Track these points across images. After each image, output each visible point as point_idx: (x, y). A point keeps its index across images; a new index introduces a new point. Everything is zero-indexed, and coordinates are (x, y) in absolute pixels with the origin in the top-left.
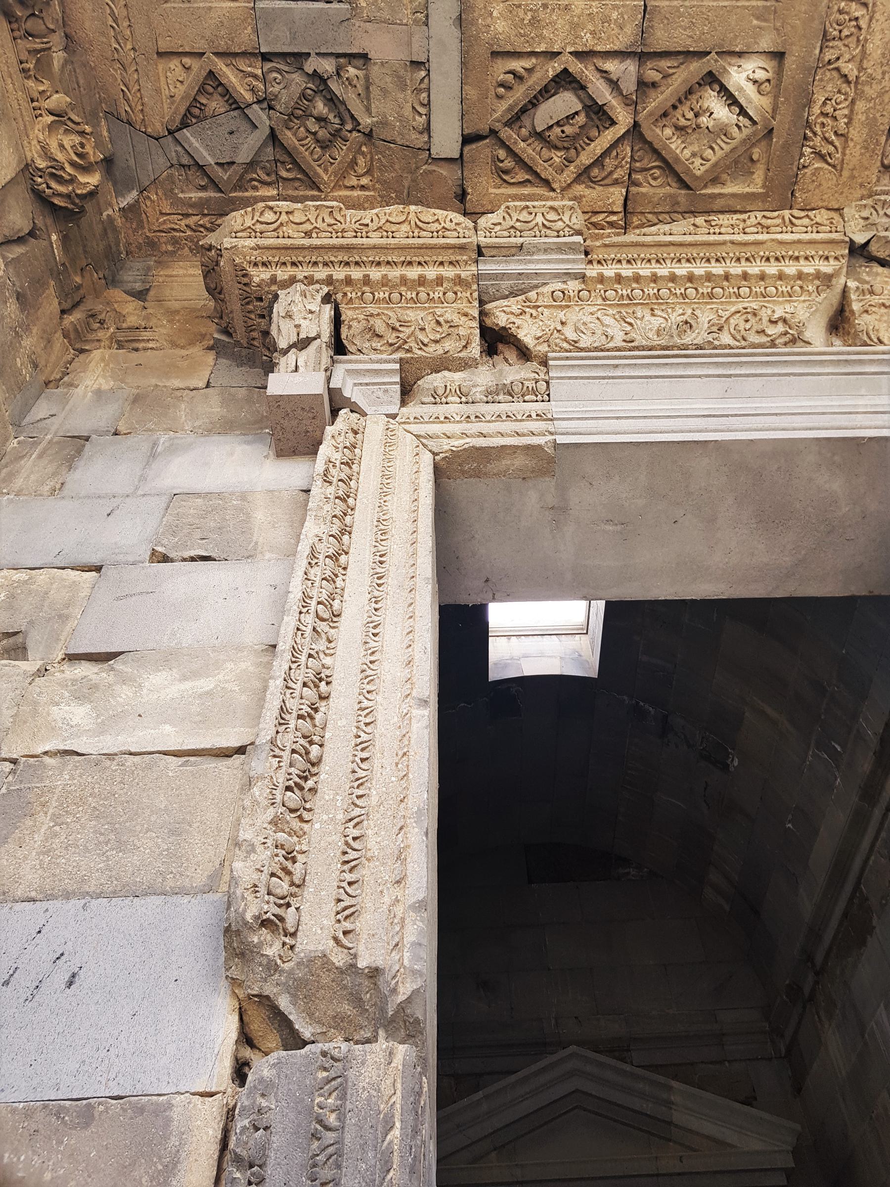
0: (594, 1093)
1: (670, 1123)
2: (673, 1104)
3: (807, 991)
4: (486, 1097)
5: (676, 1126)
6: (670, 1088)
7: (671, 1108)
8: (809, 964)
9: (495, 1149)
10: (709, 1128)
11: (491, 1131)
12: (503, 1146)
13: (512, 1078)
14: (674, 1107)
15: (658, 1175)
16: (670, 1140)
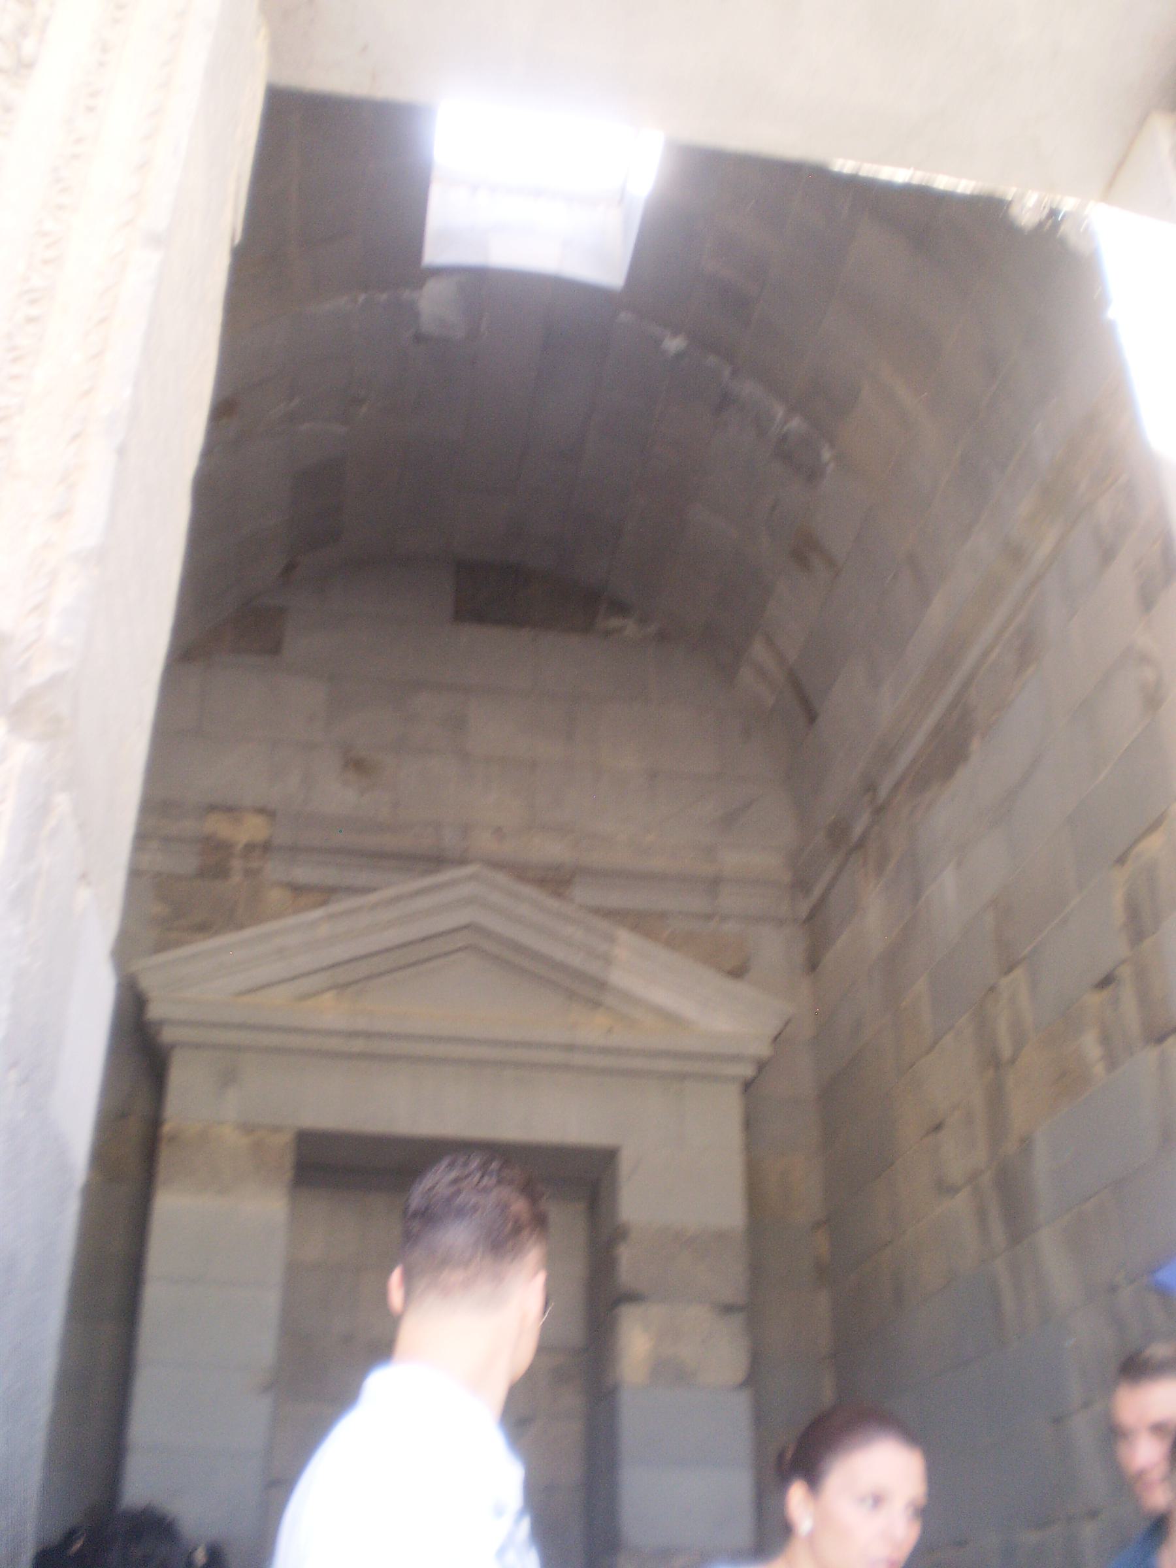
10: (661, 996)
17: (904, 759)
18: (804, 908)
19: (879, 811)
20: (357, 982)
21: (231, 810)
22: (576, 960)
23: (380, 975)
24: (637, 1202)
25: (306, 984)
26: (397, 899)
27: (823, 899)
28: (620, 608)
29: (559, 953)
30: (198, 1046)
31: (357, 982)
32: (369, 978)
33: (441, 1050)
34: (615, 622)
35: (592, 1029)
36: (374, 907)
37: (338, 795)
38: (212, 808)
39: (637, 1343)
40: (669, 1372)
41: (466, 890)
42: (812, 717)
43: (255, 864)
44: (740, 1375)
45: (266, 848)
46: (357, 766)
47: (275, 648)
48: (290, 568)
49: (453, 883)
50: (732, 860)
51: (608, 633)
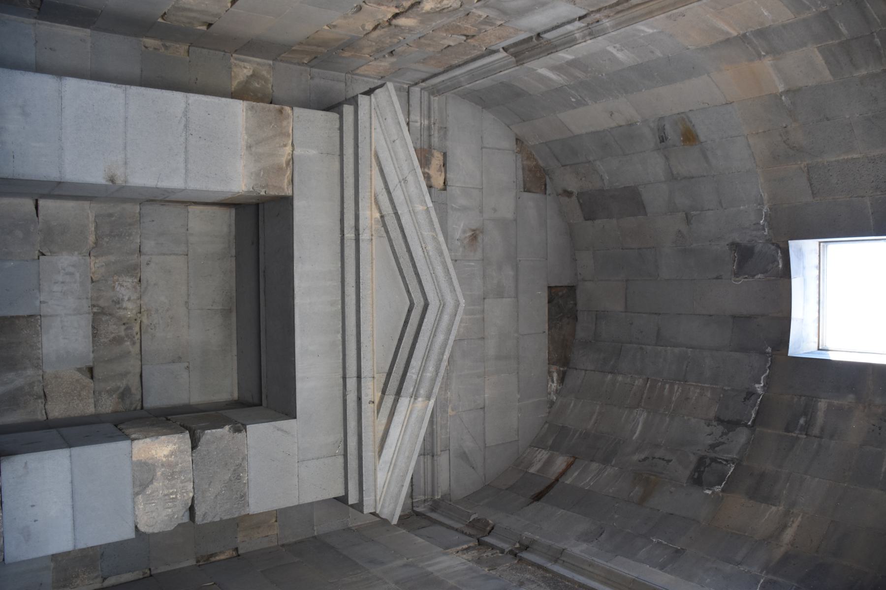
0: (426, 320)
1: (398, 393)
3: (488, 539)
5: (396, 401)
6: (428, 398)
8: (517, 545)
9: (382, 217)
11: (399, 212)
12: (384, 225)
13: (441, 238)
15: (359, 377)
17: (556, 568)
19: (514, 554)
20: (387, 232)
22: (412, 374)
24: (260, 434)
26: (441, 254)
28: (562, 379)
29: (415, 363)
30: (341, 129)
31: (387, 232)
32: (390, 240)
33: (351, 290)
34: (555, 376)
35: (371, 390)
36: (435, 238)
38: (445, 155)
39: (162, 449)
40: (144, 476)
42: (538, 497)
44: (142, 528)
46: (474, 237)
47: (527, 190)
48: (569, 194)
50: (443, 460)
51: (550, 373)
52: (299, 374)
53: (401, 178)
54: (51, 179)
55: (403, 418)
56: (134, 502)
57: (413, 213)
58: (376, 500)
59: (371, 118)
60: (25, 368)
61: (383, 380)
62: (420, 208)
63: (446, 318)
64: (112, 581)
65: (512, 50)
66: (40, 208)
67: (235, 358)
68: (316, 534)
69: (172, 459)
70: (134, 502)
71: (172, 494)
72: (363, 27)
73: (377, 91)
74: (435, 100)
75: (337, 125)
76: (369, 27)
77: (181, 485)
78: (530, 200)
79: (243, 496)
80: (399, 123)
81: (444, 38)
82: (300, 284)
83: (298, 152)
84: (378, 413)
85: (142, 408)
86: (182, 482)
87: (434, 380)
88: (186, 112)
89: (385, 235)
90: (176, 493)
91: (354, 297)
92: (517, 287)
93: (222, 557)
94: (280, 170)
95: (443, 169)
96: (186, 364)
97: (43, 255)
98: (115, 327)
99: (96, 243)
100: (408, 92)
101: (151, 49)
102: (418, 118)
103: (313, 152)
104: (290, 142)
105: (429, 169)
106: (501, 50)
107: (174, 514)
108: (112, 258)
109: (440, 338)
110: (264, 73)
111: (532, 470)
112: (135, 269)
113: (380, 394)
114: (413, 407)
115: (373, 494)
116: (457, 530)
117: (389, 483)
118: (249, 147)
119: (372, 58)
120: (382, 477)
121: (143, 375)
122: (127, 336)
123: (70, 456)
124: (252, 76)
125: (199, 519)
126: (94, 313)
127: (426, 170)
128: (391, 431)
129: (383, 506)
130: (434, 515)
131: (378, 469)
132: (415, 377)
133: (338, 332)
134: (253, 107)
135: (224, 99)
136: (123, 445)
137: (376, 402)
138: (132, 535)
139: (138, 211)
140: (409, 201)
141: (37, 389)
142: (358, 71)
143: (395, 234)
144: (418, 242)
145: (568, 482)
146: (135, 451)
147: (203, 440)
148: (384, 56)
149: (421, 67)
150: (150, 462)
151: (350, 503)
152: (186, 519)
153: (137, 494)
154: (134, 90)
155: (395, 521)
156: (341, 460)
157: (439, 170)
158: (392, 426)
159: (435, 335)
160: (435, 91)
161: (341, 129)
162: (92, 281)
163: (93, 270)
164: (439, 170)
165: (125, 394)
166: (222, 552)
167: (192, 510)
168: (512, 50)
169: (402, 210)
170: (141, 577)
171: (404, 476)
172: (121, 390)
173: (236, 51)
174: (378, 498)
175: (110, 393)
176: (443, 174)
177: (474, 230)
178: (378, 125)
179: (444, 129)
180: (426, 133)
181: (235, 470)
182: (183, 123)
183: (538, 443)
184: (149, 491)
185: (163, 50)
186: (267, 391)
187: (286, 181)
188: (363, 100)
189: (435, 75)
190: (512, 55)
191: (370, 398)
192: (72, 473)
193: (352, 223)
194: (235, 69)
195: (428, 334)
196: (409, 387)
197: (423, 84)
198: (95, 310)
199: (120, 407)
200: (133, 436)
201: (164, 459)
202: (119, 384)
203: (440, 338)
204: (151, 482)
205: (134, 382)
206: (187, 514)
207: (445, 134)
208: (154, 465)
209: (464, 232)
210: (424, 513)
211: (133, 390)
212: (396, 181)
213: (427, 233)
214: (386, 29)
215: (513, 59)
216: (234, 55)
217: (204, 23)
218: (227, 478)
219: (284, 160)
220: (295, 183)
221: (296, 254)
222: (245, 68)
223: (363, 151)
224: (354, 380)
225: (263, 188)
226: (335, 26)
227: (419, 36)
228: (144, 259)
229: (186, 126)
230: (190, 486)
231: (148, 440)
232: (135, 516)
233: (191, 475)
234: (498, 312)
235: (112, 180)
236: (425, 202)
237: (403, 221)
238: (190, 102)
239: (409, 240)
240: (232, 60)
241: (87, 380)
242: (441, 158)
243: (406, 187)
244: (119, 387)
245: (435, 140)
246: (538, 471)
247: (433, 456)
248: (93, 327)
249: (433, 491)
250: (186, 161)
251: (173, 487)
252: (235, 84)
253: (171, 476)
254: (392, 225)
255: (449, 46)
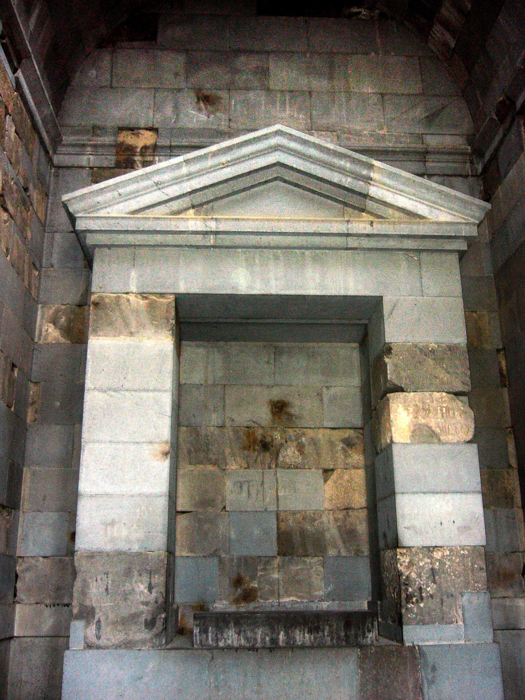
0: (295, 166)
1: (366, 196)
2: (371, 180)
4: (187, 162)
5: (372, 199)
6: (371, 167)
7: (370, 184)
9: (193, 207)
11: (189, 190)
12: (201, 205)
14: (372, 182)
15: (348, 235)
16: (363, 210)
18: (480, 168)
20: (208, 202)
21: (133, 130)
22: (347, 181)
23: (222, 198)
25: (175, 205)
26: (229, 149)
27: (494, 156)
29: (336, 178)
30: (109, 247)
31: (208, 202)
33: (265, 240)
36: (215, 154)
37: (195, 117)
38: (121, 129)
39: (401, 418)
41: (273, 141)
43: (149, 159)
44: (470, 436)
45: (155, 147)
46: (206, 100)
49: (266, 137)
50: (433, 141)
51: (351, 16)
52: (342, 293)
53: (156, 188)
54: (166, 503)
55: (388, 193)
56: (446, 443)
57: (190, 176)
58: (465, 224)
59: (98, 218)
60: (322, 523)
61: (350, 210)
62: (185, 170)
63: (293, 145)
64: (513, 462)
65: (16, 64)
66: (183, 510)
67: (320, 344)
68: (492, 275)
69: (411, 409)
70: (446, 443)
71: (441, 410)
72: (6, 222)
73: (71, 210)
74: (67, 139)
75: (106, 250)
76: (5, 216)
77: (435, 402)
78: (167, 34)
79: (452, 349)
80: (101, 189)
81: (10, 138)
82: (258, 289)
83: (133, 288)
84: (382, 217)
85: (362, 428)
86: (433, 402)
87: (354, 161)
88: (101, 390)
89: (211, 204)
90: (440, 407)
91: (270, 237)
92: (258, 52)
93: (503, 363)
94: (152, 306)
95: (136, 132)
96: (325, 390)
97: (225, 507)
98: (288, 450)
99: (215, 463)
100: (59, 167)
101: (36, 416)
102: (85, 158)
103: (133, 274)
104: (125, 296)
105: (136, 147)
106: (16, 75)
107: (459, 409)
108: (228, 451)
109: (313, 152)
110: (51, 312)
111: (452, 44)
112: (237, 431)
113: (364, 214)
114: (380, 183)
115: (460, 226)
116: (505, 135)
117: (451, 209)
118: (131, 334)
119: (31, 208)
120: (444, 217)
121: (332, 426)
122: (296, 440)
123: (402, 493)
124: (55, 324)
125: (467, 389)
126: (277, 466)
127: (138, 150)
128: (400, 205)
129: (472, 217)
130: (487, 156)
131: (436, 220)
132: (349, 179)
133: (304, 253)
134: (94, 330)
135: (89, 357)
136: (396, 450)
137: (371, 218)
138: (474, 448)
139: (185, 428)
140: (177, 180)
141: (340, 516)
142: (43, 221)
143: (210, 195)
144: (218, 172)
145: (469, 6)
146: (402, 441)
147: (397, 382)
148: (28, 196)
149: (35, 157)
150: (412, 428)
151: (465, 248)
152: (465, 399)
153: (439, 440)
154: (85, 435)
155: (488, 206)
156: (424, 256)
157: (137, 135)
158: (396, 204)
159: (310, 157)
160: (57, 141)
161: (109, 247)
162: (248, 467)
163: (238, 467)
164: (137, 135)
165: (349, 443)
166: (499, 363)
167: (457, 394)
168: (16, 64)
169: (187, 186)
170: (513, 436)
171: (447, 195)
172: (345, 446)
173: (33, 339)
174: (463, 221)
175: (347, 456)
176: (141, 131)
177: (198, 99)
178: (105, 210)
179: (95, 130)
180: (100, 150)
181: (426, 355)
182: (113, 393)
183: (424, 32)
184: (438, 430)
185: (36, 405)
186: (357, 323)
187: (161, 300)
188: (81, 225)
189: (42, 142)
190: (19, 63)
191: (368, 226)
192: (417, 493)
193: (200, 237)
194: (50, 339)
195: (308, 164)
196: (358, 186)
197: (51, 152)
198: (274, 466)
199: (360, 447)
200: (388, 441)
201: (411, 416)
202: (339, 448)
203: (313, 152)
204: (430, 428)
205: (337, 435)
206: (461, 398)
207: (99, 128)
208: (415, 425)
209: (200, 110)
210: (484, 175)
211: (346, 435)
212: (158, 193)
213: (210, 162)
214: (6, 198)
215: (24, 61)
216: (36, 340)
217: (13, 370)
218: (431, 362)
219: (142, 302)
220: (163, 291)
221: (229, 292)
222: (47, 330)
223: (130, 225)
224: (349, 239)
225: (168, 321)
226: (7, 249)
227: (9, 165)
228: (228, 423)
229: (115, 391)
230: (436, 395)
231: (393, 429)
232: (458, 443)
233: (427, 394)
234: (283, 74)
235: (166, 454)
236: (178, 164)
237: (198, 187)
238: (93, 387)
239: (216, 181)
240: (41, 342)
241: (334, 476)
242: (124, 133)
243: (164, 183)
244: (343, 449)
245: (108, 140)
246: (454, 38)
247: (427, 152)
248: (289, 468)
249: (462, 154)
250: (147, 390)
251: (436, 410)
252: (62, 340)
253: (427, 410)
254: (204, 200)
255: (16, 132)
